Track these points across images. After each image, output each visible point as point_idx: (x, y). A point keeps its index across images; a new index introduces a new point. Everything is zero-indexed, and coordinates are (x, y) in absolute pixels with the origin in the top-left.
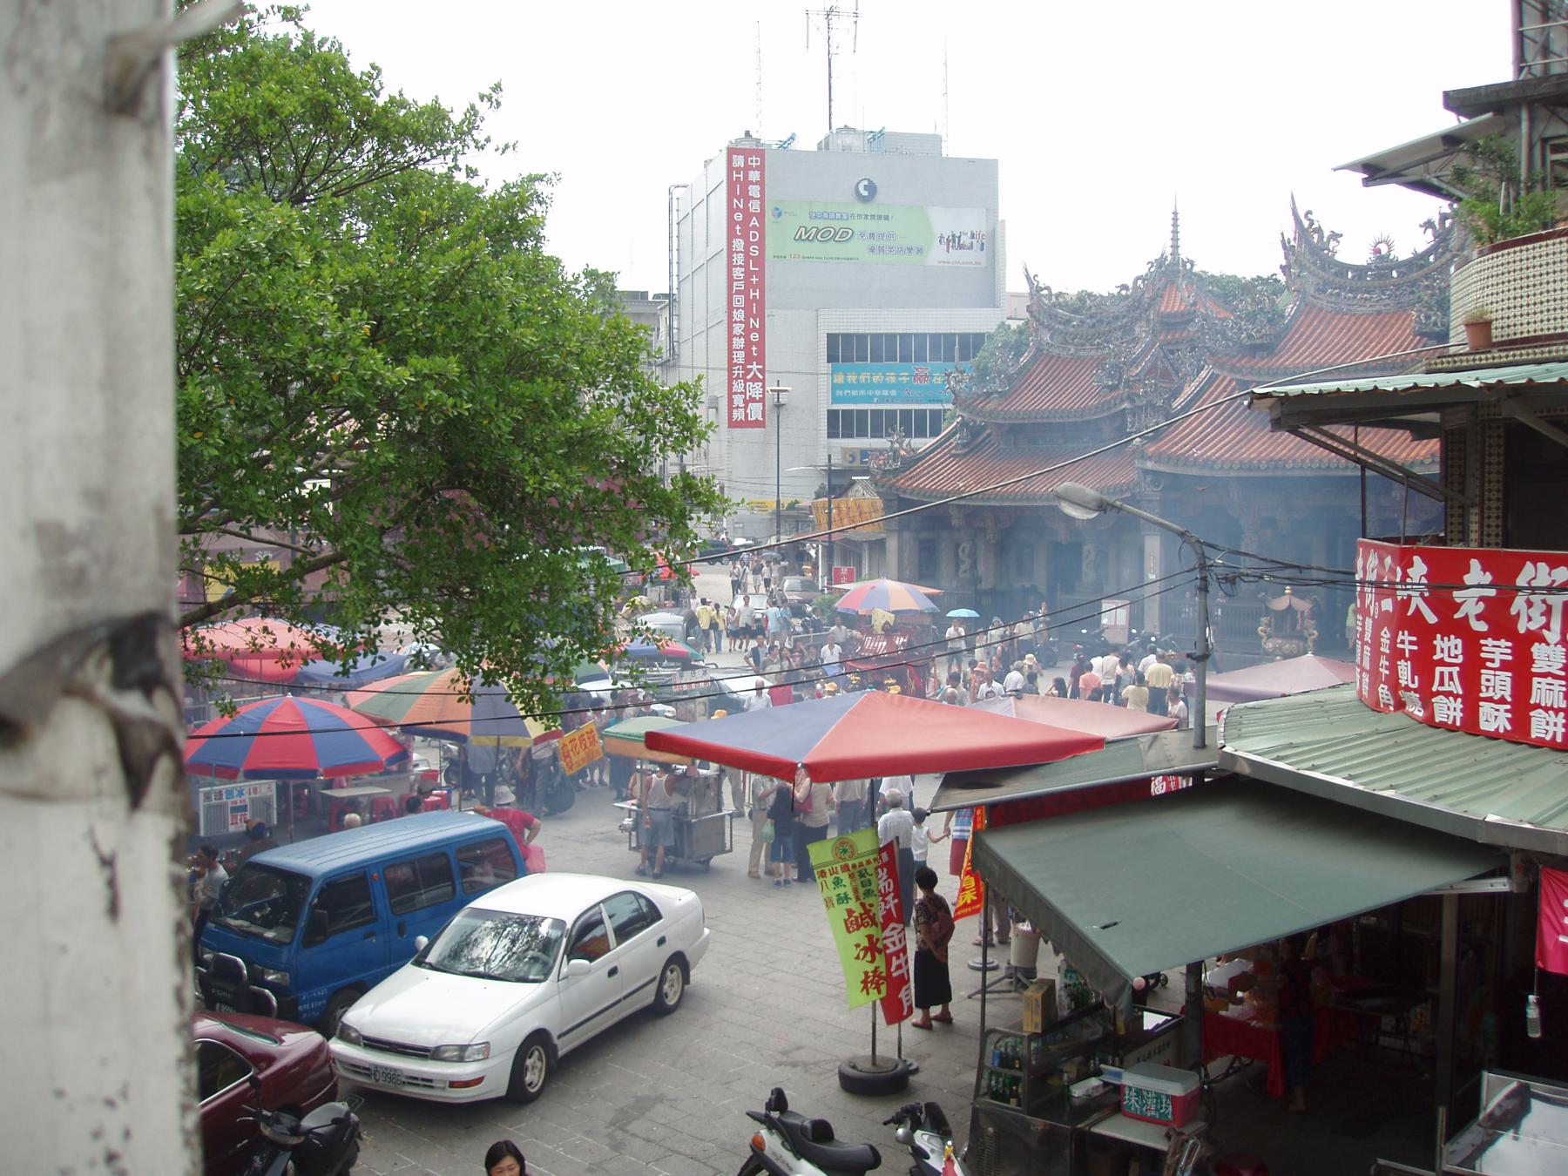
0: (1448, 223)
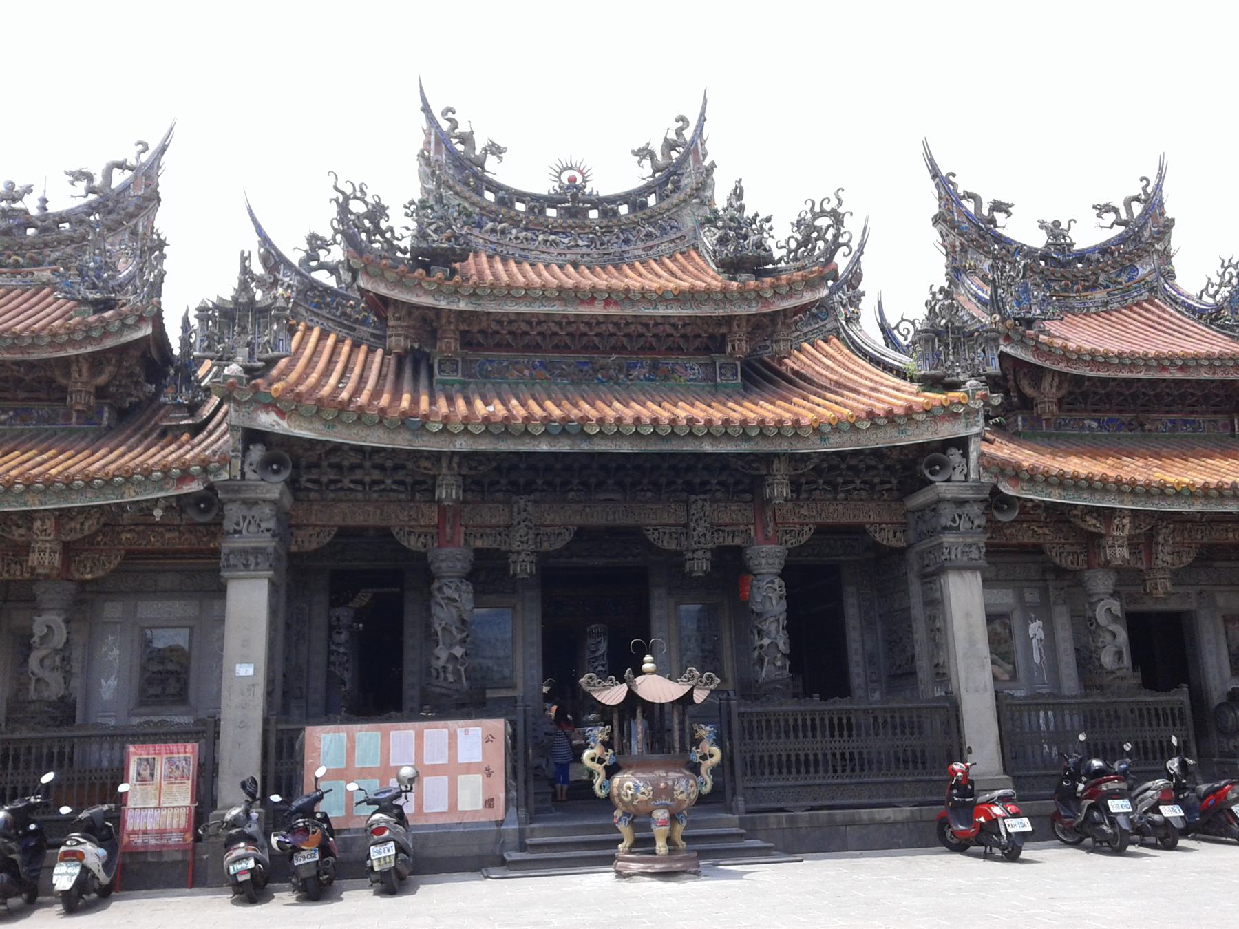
0: (674, 155)
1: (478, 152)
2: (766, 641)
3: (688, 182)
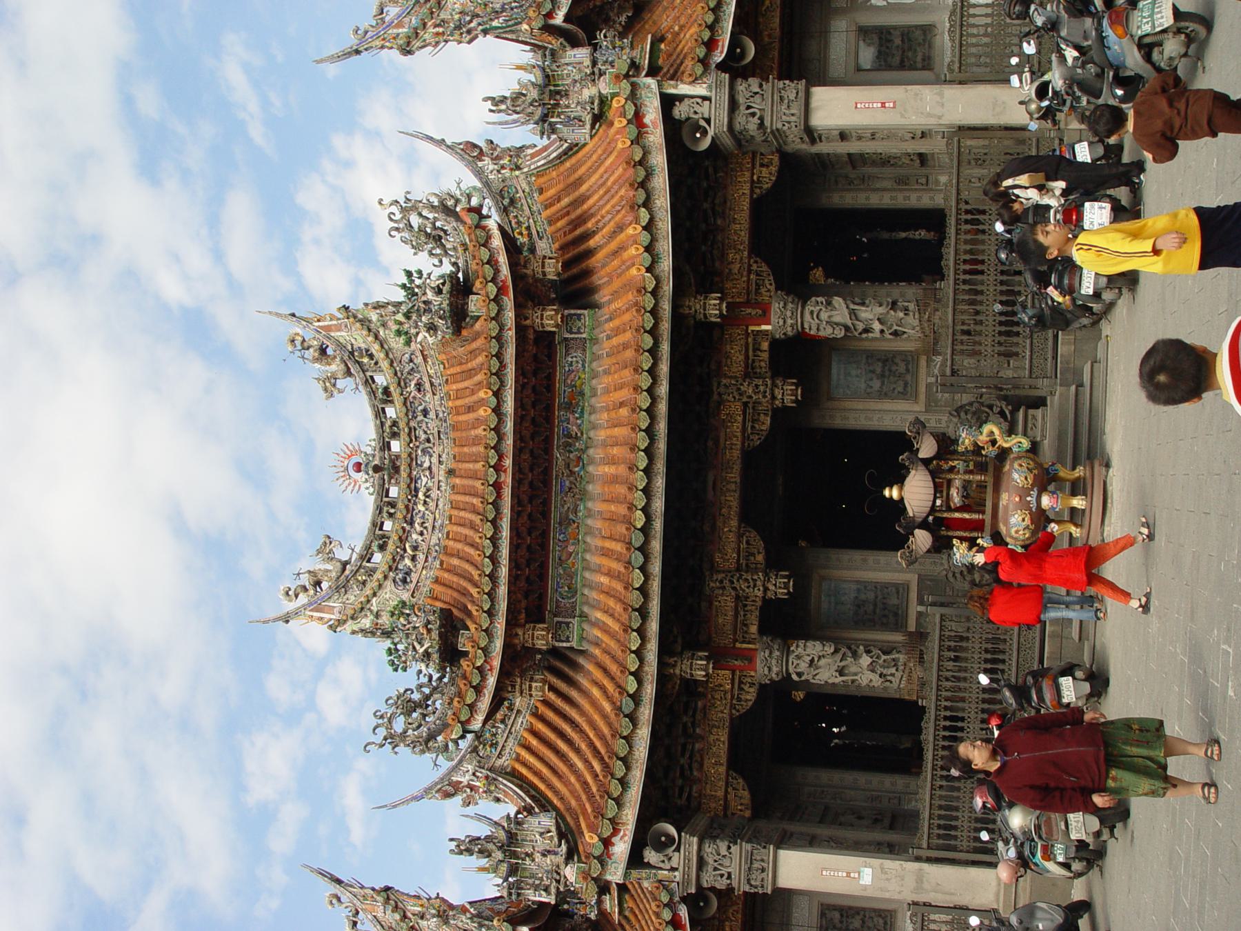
1: (329, 567)
2: (877, 326)
3: (358, 338)
